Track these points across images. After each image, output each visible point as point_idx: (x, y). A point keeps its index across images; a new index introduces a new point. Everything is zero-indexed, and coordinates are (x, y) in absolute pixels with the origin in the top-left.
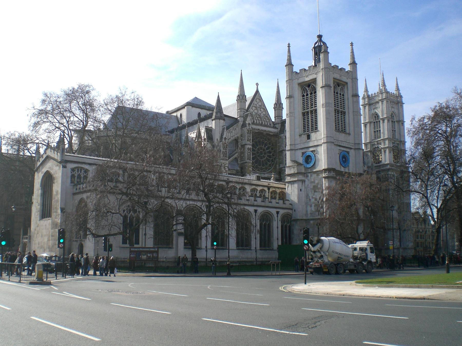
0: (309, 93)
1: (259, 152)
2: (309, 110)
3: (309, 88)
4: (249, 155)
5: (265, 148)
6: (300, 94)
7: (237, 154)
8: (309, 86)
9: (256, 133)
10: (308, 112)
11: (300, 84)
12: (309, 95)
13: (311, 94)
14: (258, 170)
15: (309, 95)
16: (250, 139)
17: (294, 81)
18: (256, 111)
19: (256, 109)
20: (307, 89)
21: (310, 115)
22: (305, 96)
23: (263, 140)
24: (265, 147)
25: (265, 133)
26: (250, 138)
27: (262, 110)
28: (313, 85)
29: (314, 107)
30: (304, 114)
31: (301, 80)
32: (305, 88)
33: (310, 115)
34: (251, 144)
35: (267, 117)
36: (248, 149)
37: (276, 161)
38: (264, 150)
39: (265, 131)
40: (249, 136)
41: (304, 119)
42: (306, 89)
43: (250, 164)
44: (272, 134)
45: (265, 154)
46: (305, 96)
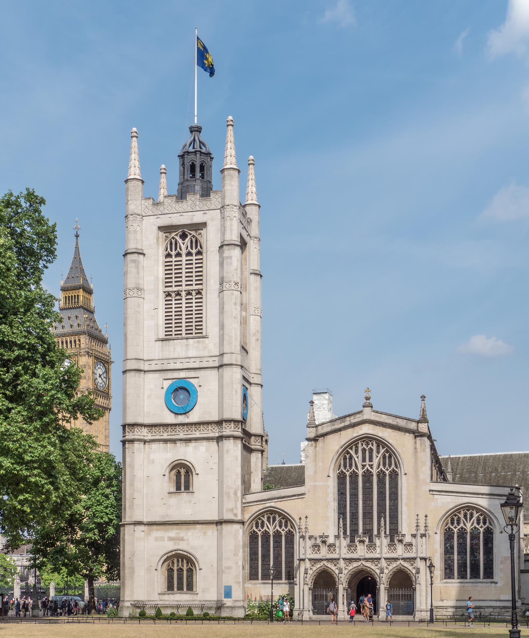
0: (184, 252)
2: (184, 288)
3: (184, 240)
6: (161, 252)
8: (184, 236)
10: (178, 294)
11: (160, 228)
12: (184, 258)
13: (189, 254)
15: (184, 258)
17: (144, 218)
20: (180, 241)
21: (184, 301)
22: (174, 257)
28: (194, 236)
29: (194, 285)
30: (168, 294)
31: (165, 221)
32: (173, 238)
33: (184, 301)
41: (168, 307)
42: (176, 244)
46: (174, 257)
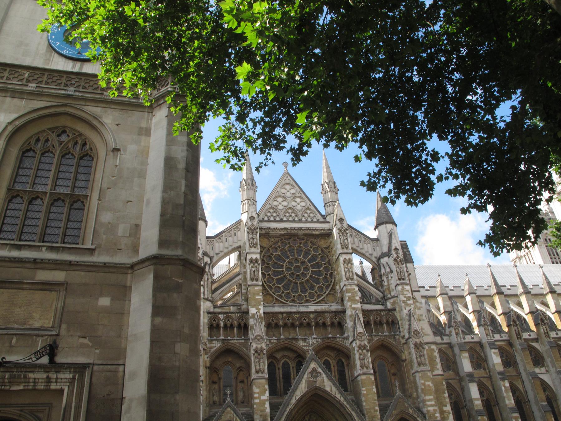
1: (292, 267)
4: (254, 272)
5: (306, 260)
7: (240, 277)
9: (282, 235)
14: (293, 301)
16: (256, 244)
18: (285, 203)
19: (283, 199)
23: (300, 247)
24: (305, 256)
25: (300, 233)
26: (255, 241)
27: (298, 200)
34: (259, 251)
35: (308, 209)
36: (251, 261)
37: (333, 280)
38: (303, 263)
39: (300, 229)
40: (253, 239)
43: (257, 288)
44: (317, 233)
45: (306, 269)
